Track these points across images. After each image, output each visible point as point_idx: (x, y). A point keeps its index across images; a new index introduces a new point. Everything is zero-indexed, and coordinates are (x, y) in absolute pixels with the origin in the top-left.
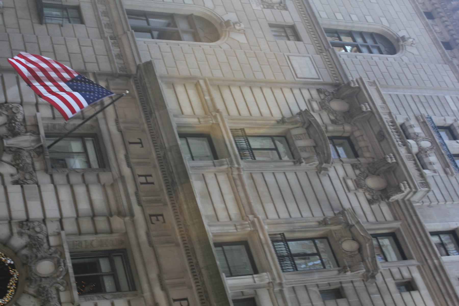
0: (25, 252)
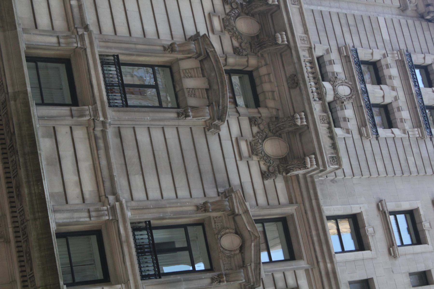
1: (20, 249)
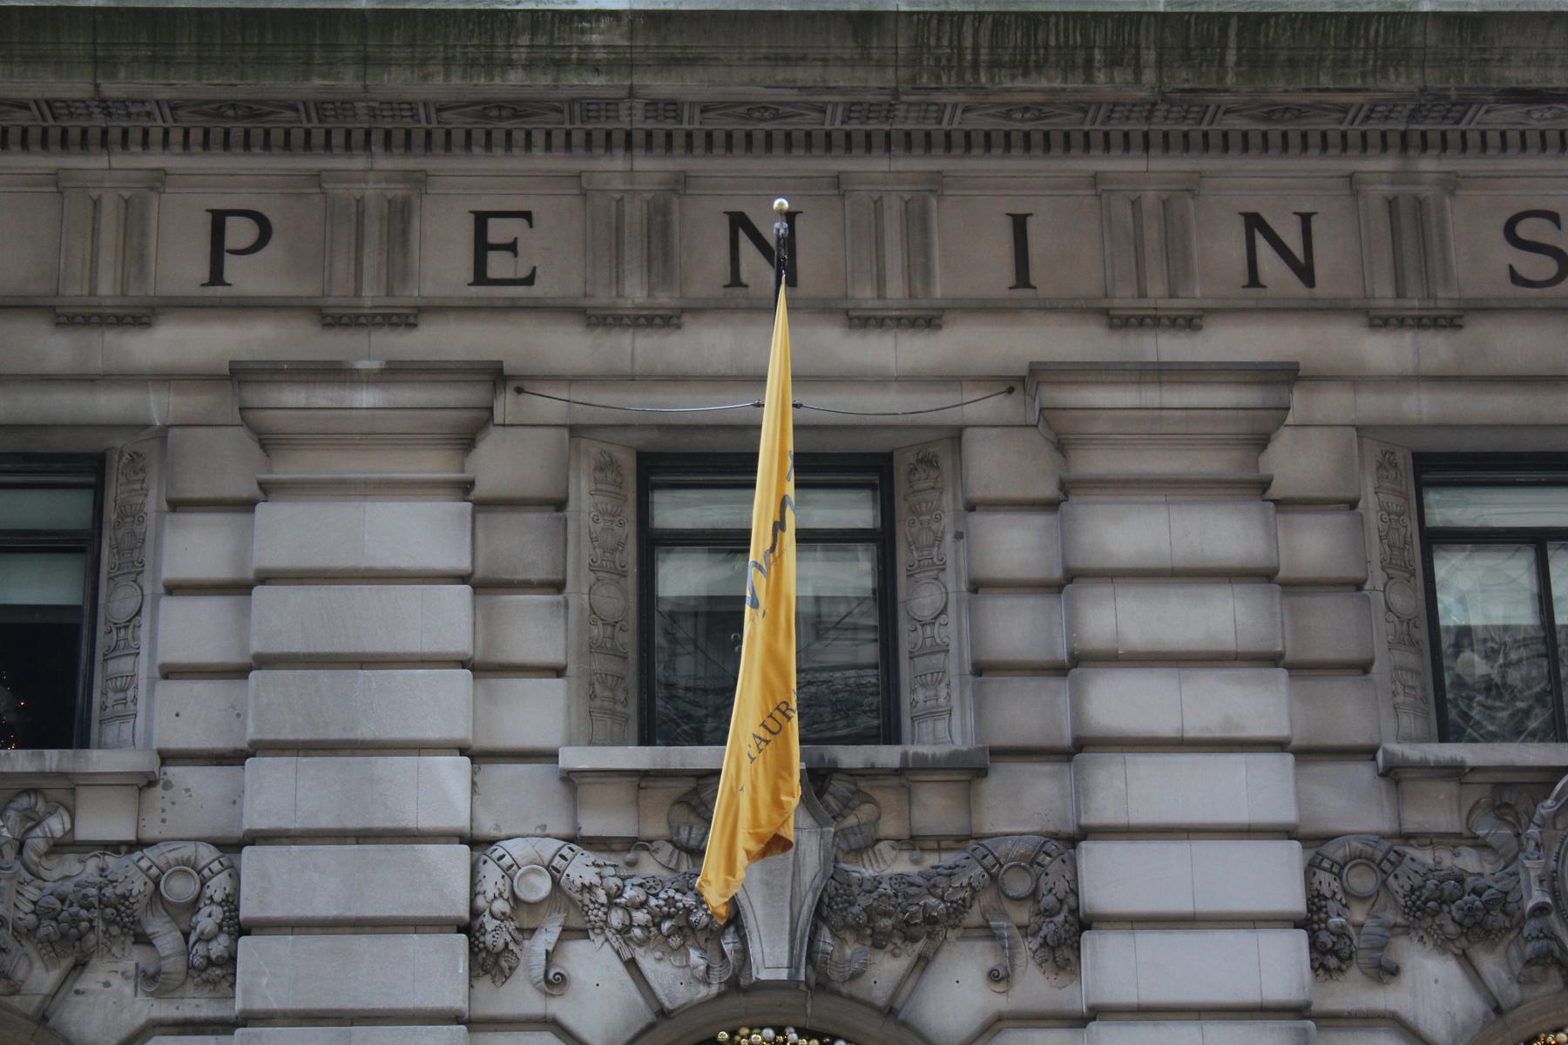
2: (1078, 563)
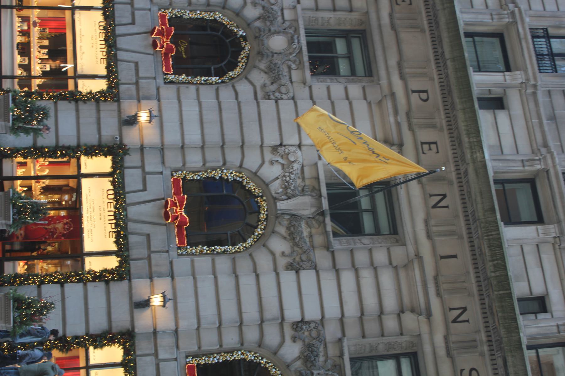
0: (258, 24)
1: (433, 36)
2: (378, 269)
